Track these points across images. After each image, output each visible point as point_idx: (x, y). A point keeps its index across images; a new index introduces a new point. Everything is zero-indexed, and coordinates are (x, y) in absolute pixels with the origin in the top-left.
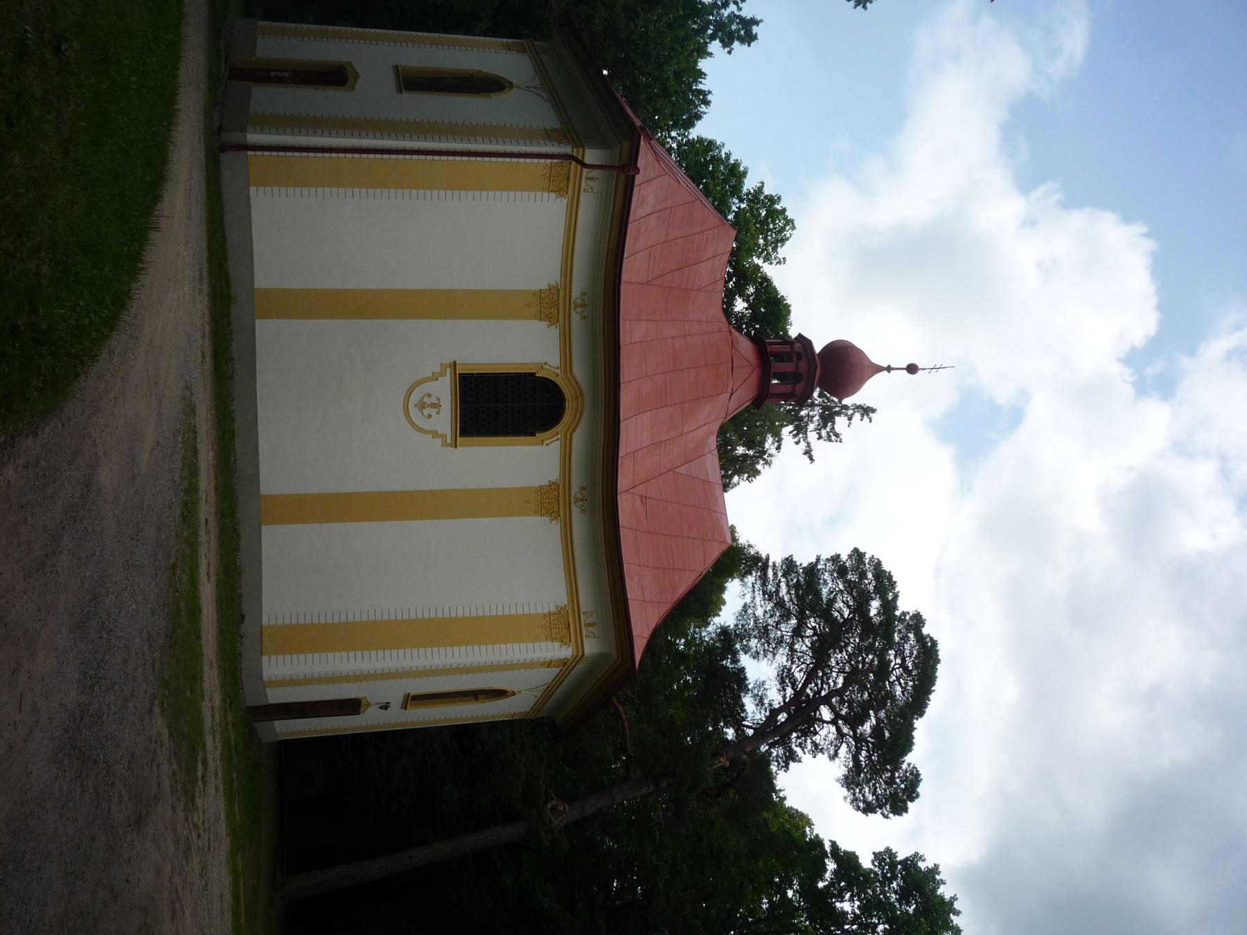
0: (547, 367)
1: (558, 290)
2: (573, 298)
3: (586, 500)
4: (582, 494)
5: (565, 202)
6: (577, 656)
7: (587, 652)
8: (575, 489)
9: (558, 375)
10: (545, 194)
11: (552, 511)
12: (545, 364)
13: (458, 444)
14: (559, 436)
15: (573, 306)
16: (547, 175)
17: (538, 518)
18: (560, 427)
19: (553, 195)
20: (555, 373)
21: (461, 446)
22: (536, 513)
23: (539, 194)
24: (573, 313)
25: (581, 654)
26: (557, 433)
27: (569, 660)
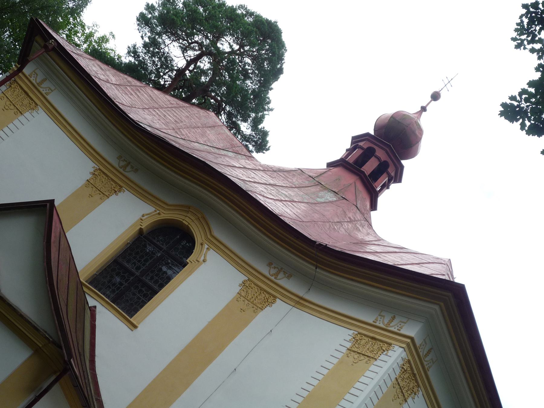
0: (146, 217)
1: (99, 169)
2: (116, 166)
3: (282, 269)
4: (275, 268)
5: (41, 111)
6: (408, 345)
7: (412, 334)
8: (265, 270)
9: (159, 214)
10: (21, 118)
11: (266, 300)
12: (143, 216)
13: (135, 323)
14: (206, 246)
15: (121, 170)
16: (8, 103)
17: (262, 315)
18: (199, 237)
19: (27, 114)
20: (156, 214)
21: (139, 323)
22: (256, 312)
23: (16, 122)
24: (127, 174)
25: (409, 341)
26: (202, 244)
27: (409, 361)
